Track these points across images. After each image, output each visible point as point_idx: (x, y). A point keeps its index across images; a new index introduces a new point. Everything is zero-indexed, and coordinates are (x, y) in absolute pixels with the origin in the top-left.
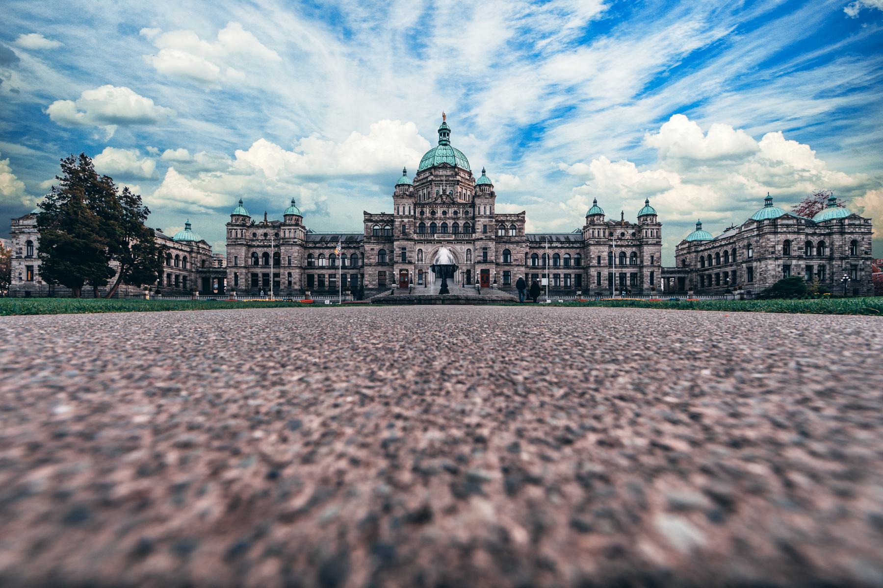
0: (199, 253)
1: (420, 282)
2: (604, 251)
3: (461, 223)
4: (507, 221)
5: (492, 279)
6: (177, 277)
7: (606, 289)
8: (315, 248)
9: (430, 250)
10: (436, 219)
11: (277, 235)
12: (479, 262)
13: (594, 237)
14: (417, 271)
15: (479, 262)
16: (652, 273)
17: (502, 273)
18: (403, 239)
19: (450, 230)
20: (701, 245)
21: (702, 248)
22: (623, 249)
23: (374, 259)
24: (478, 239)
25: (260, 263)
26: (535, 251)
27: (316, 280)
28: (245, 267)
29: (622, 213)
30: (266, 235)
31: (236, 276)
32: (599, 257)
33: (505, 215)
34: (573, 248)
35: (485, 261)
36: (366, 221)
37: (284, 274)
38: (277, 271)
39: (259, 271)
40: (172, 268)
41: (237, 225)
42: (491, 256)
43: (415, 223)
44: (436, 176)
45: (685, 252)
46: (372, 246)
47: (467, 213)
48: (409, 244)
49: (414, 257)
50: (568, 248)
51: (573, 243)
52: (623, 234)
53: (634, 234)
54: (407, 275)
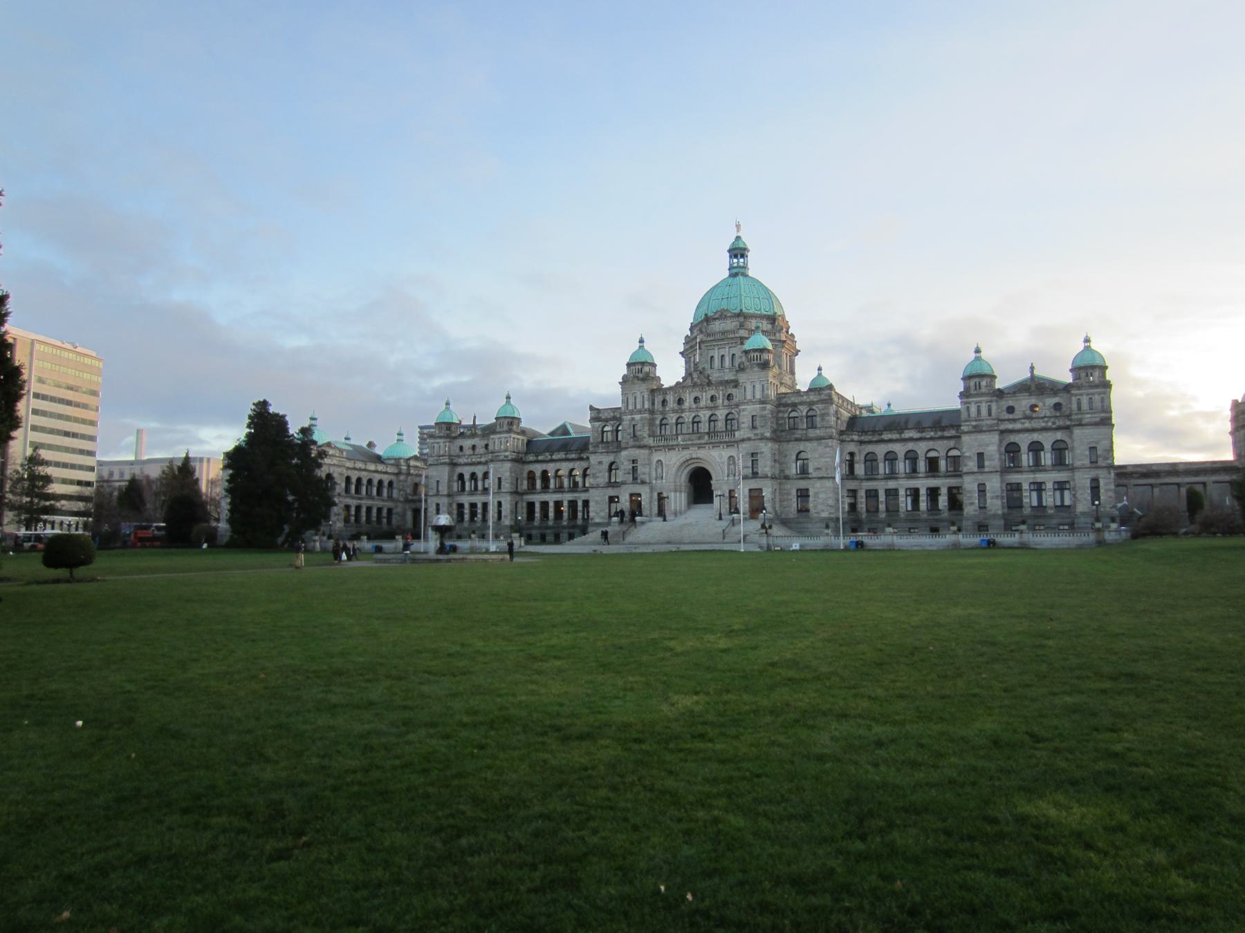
0: (408, 474)
2: (991, 445)
3: (721, 414)
6: (380, 510)
8: (537, 462)
10: (683, 411)
11: (487, 446)
12: (745, 478)
15: (745, 478)
17: (794, 492)
18: (634, 447)
19: (704, 427)
22: (1036, 437)
23: (603, 478)
24: (743, 440)
25: (467, 488)
26: (870, 448)
28: (449, 495)
30: (474, 447)
35: (755, 475)
36: (593, 420)
39: (466, 500)
40: (372, 498)
41: (440, 437)
42: (765, 466)
47: (729, 397)
48: (641, 454)
51: (943, 429)
52: (1033, 407)
53: (1057, 406)
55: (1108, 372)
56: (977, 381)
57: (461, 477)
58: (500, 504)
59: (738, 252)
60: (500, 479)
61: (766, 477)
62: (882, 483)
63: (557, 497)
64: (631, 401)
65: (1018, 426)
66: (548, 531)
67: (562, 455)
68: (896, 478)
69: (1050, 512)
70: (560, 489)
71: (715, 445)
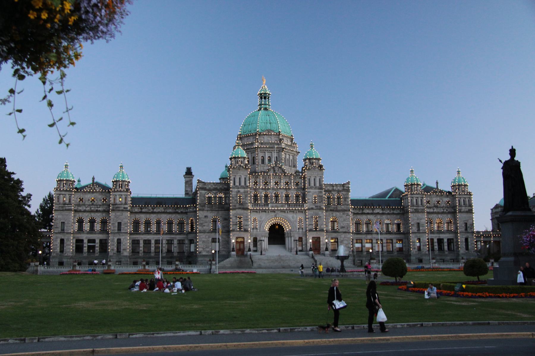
1: (255, 249)
4: (333, 190)
5: (323, 247)
7: (426, 255)
8: (141, 212)
9: (263, 218)
10: (268, 189)
13: (412, 205)
14: (252, 239)
15: (310, 230)
16: (466, 240)
18: (240, 208)
27: (142, 244)
29: (437, 183)
31: (62, 241)
32: (418, 224)
33: (332, 185)
34: (393, 214)
38: (103, 236)
39: (85, 237)
41: (66, 190)
43: (251, 192)
44: (262, 144)
46: (205, 213)
50: (388, 214)
52: (438, 202)
54: (243, 242)
57: (80, 222)
60: (120, 224)
61: (322, 230)
62: (364, 236)
65: (432, 210)
66: (151, 260)
67: (161, 209)
68: (372, 234)
69: (446, 253)
71: (292, 211)
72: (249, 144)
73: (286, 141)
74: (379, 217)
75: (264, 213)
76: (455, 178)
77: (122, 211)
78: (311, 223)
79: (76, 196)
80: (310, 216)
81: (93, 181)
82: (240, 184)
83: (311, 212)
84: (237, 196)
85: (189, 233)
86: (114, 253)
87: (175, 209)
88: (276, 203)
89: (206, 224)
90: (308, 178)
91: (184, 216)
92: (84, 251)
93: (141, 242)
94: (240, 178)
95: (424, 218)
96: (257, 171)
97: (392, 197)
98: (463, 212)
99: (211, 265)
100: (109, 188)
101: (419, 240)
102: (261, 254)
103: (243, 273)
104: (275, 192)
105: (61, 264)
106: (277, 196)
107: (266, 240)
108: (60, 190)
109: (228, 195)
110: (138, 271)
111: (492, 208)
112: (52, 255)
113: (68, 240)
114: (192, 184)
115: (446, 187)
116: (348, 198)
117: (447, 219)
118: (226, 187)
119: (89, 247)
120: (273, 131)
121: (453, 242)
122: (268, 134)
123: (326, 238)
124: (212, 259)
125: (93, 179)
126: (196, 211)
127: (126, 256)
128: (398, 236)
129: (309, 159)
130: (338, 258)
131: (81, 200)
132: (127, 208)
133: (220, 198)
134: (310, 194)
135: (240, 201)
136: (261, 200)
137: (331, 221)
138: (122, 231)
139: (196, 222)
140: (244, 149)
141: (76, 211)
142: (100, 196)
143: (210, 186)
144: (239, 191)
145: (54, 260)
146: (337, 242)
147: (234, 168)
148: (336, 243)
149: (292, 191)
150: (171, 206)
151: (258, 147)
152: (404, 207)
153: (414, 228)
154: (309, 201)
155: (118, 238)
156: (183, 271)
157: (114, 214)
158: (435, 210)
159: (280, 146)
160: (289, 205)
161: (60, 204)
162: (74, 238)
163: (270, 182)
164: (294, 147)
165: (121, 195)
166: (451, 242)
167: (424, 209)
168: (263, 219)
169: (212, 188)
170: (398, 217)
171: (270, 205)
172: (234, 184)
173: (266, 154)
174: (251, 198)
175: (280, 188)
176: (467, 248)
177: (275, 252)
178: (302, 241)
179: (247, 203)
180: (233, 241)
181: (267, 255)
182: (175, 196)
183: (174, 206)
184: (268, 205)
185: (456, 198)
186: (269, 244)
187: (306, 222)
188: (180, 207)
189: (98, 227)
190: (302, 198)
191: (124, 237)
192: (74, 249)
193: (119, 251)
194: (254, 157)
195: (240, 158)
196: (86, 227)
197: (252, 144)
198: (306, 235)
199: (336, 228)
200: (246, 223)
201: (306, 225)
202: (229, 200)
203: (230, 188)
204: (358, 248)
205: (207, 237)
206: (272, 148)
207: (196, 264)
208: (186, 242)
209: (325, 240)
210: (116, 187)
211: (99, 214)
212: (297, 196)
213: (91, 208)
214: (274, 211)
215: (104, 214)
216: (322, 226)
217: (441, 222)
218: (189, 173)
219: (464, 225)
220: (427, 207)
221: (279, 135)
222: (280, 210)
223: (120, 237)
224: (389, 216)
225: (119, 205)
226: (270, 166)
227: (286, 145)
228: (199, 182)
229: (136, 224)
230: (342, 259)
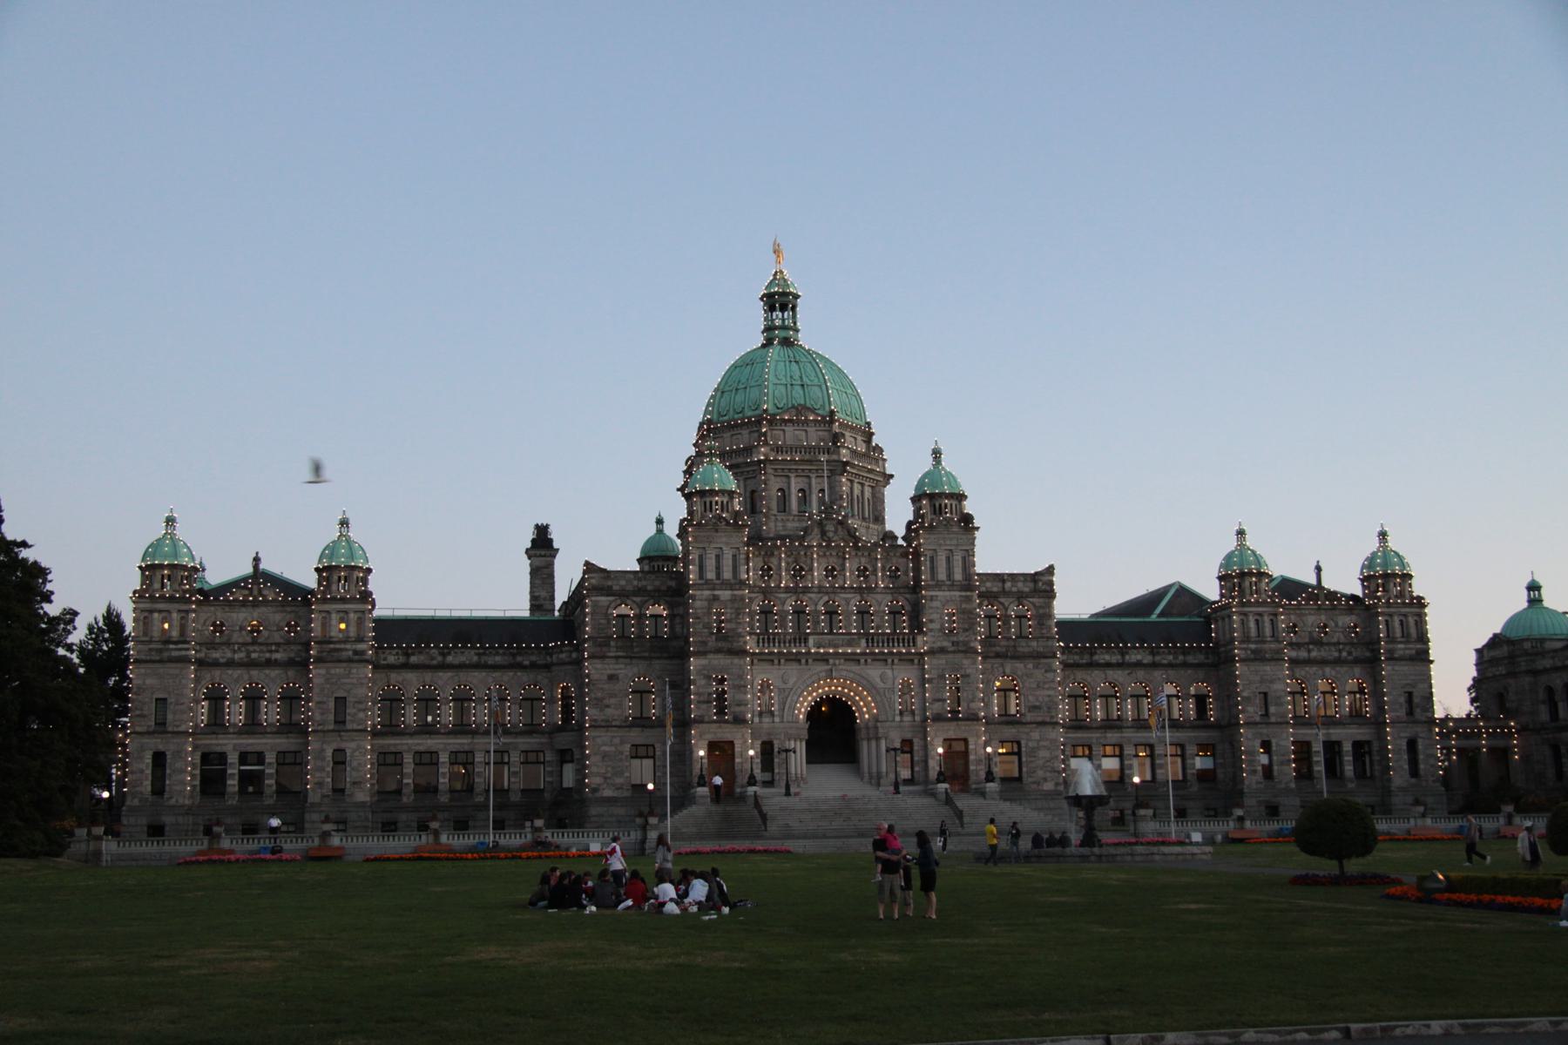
1: (767, 777)
4: (1004, 593)
5: (977, 770)
8: (406, 666)
9: (792, 681)
10: (806, 590)
13: (1246, 639)
14: (758, 744)
15: (938, 718)
16: (1412, 745)
18: (718, 651)
20: (1543, 654)
21: (1547, 663)
27: (409, 768)
29: (1318, 569)
31: (159, 759)
34: (1185, 665)
37: (320, 755)
38: (286, 743)
39: (230, 746)
41: (172, 599)
44: (778, 449)
45: (1502, 670)
46: (610, 667)
49: (753, 702)
50: (1171, 665)
55: (1414, 582)
56: (1241, 576)
58: (339, 752)
59: (779, 301)
60: (341, 702)
61: (973, 718)
63: (462, 742)
64: (710, 563)
65: (1303, 654)
67: (470, 656)
68: (1120, 728)
69: (1351, 786)
70: (461, 728)
71: (882, 659)
72: (739, 452)
73: (852, 443)
74: (1141, 674)
75: (795, 666)
76: (1374, 555)
77: (350, 661)
78: (938, 696)
79: (203, 616)
80: (934, 674)
81: (256, 567)
82: (718, 577)
83: (941, 660)
84: (709, 613)
85: (556, 730)
86: (324, 796)
87: (514, 655)
88: (831, 632)
89: (613, 701)
90: (929, 554)
91: (542, 677)
92: (230, 789)
93: (408, 759)
94: (718, 557)
95: (1283, 680)
96: (764, 535)
97: (1171, 615)
98: (1401, 659)
99: (644, 828)
100: (305, 592)
101: (1266, 745)
102: (788, 794)
103: (752, 851)
104: (826, 598)
105: (156, 831)
106: (831, 613)
107: (801, 748)
108: (152, 597)
109: (681, 610)
110: (417, 849)
111: (1479, 646)
112: (128, 803)
113: (179, 754)
114: (551, 576)
115: (1345, 580)
116: (1050, 616)
117: (1352, 683)
118: (673, 584)
119: (245, 778)
120: (813, 411)
121: (1370, 753)
122: (798, 422)
123: (986, 744)
124: (646, 810)
125: (257, 560)
126: (579, 662)
127: (363, 804)
128: (1203, 735)
129: (932, 497)
130: (1077, 801)
131: (218, 628)
132: (363, 653)
133: (656, 617)
134: (935, 604)
135: (719, 629)
136: (783, 625)
137: (999, 690)
138: (349, 726)
139: (581, 695)
140: (730, 468)
141: (200, 663)
142: (278, 617)
143: (623, 583)
144: (716, 598)
145: (132, 820)
146: (1019, 754)
147: (699, 524)
148: (1015, 758)
149: (879, 597)
150: (501, 647)
151: (767, 460)
152: (1217, 644)
153: (1250, 709)
154: (931, 626)
155: (335, 746)
156: (558, 847)
157: (323, 672)
158: (1312, 654)
159: (835, 457)
160: (871, 639)
161: (150, 642)
162: (195, 747)
163: (811, 569)
164: (877, 460)
165: (346, 612)
166: (1363, 755)
167: (1280, 651)
168: (790, 685)
169: (630, 588)
170: (1201, 674)
171: (811, 641)
172: (701, 577)
173: (793, 480)
174: (752, 619)
175: (842, 588)
176: (1414, 772)
177: (827, 785)
178: (911, 752)
179: (740, 635)
180: (702, 753)
181: (804, 794)
182: (509, 614)
183: (510, 647)
184: (806, 641)
185: (1378, 614)
186: (808, 762)
187: (925, 690)
188: (528, 647)
189: (270, 713)
190: (910, 619)
191: (353, 745)
192: (197, 782)
193: (339, 791)
194: (753, 492)
195: (716, 493)
196: (236, 713)
197: (749, 450)
198: (925, 735)
199: (1013, 711)
200: (739, 697)
201: (924, 700)
202: (686, 625)
203: (689, 587)
204: (1108, 772)
205: (617, 741)
206: (810, 462)
207: (581, 826)
208: (549, 756)
209: (986, 748)
210: (328, 587)
211: (274, 673)
212: (894, 613)
213: (249, 653)
214: (824, 659)
215: (291, 673)
216: (973, 705)
217: (1333, 693)
218: (542, 545)
219: (1402, 700)
220: (1291, 644)
221: (832, 421)
222: (844, 654)
223: (343, 745)
224: (1171, 672)
225: (340, 642)
226: (810, 518)
227: (854, 452)
228: (590, 568)
229: (392, 702)
230: (1087, 804)
